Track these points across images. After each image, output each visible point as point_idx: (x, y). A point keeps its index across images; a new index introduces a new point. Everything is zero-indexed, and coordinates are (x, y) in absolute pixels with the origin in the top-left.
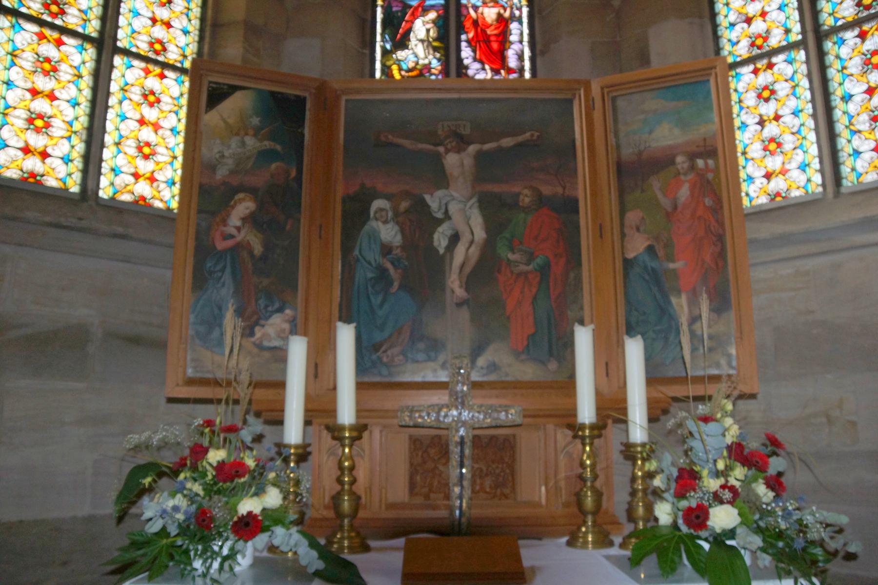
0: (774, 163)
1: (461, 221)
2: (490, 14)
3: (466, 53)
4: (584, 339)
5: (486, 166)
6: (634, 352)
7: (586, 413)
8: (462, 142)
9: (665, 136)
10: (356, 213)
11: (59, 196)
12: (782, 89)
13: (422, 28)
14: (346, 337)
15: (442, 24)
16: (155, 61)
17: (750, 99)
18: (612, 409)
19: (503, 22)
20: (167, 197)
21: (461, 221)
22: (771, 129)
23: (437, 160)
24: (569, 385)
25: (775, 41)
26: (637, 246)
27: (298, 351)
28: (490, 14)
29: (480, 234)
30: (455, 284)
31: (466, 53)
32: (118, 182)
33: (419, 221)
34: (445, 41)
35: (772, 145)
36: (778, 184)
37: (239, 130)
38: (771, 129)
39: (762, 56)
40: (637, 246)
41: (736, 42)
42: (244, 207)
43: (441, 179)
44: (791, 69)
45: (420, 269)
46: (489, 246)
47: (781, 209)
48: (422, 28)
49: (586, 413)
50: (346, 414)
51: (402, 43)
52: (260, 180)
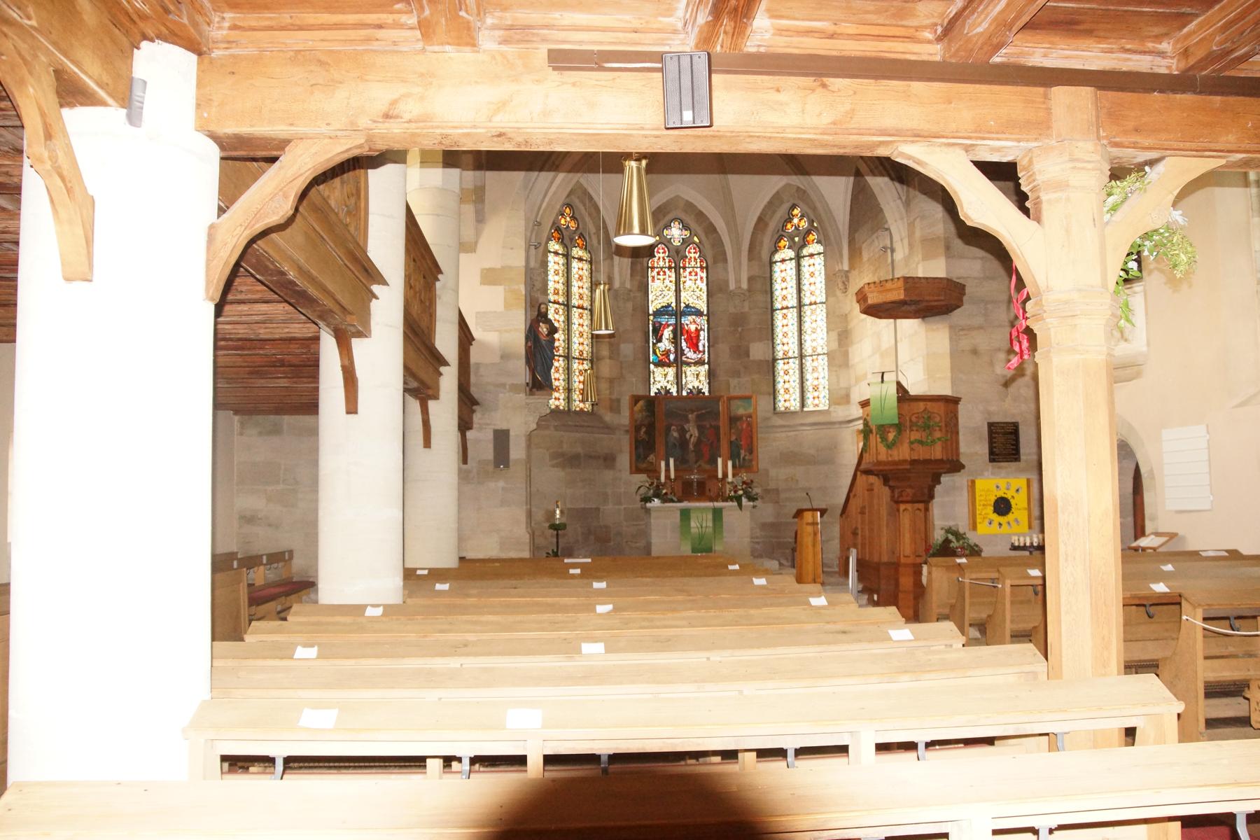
0: (787, 397)
1: (693, 432)
2: (693, 328)
3: (684, 344)
4: (720, 461)
5: (698, 416)
6: (730, 464)
7: (720, 475)
8: (692, 411)
9: (741, 411)
10: (668, 429)
11: (563, 412)
12: (791, 372)
13: (667, 333)
14: (672, 461)
15: (674, 332)
16: (581, 359)
17: (782, 373)
18: (725, 475)
19: (698, 331)
20: (587, 406)
21: (693, 432)
22: (787, 385)
23: (686, 417)
24: (717, 471)
25: (790, 354)
26: (733, 438)
27: (663, 464)
28: (693, 328)
29: (696, 433)
30: (691, 446)
31: (684, 344)
32: (578, 405)
33: (683, 431)
34: (675, 340)
35: (787, 391)
36: (787, 404)
37: (641, 411)
38: (787, 385)
39: (786, 358)
40: (733, 438)
41: (780, 350)
42: (644, 430)
43: (688, 421)
44: (794, 365)
45: (683, 443)
46: (699, 438)
47: (787, 413)
48: (667, 333)
49: (720, 475)
50: (672, 476)
51: (660, 340)
52: (646, 422)
